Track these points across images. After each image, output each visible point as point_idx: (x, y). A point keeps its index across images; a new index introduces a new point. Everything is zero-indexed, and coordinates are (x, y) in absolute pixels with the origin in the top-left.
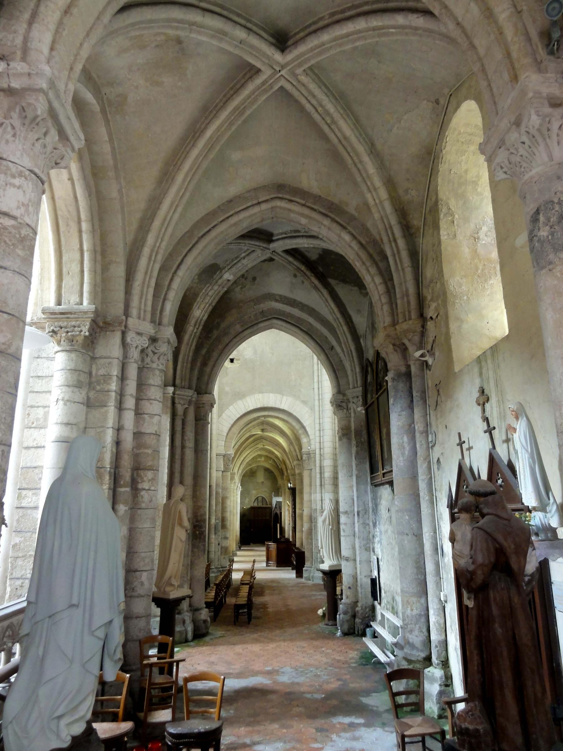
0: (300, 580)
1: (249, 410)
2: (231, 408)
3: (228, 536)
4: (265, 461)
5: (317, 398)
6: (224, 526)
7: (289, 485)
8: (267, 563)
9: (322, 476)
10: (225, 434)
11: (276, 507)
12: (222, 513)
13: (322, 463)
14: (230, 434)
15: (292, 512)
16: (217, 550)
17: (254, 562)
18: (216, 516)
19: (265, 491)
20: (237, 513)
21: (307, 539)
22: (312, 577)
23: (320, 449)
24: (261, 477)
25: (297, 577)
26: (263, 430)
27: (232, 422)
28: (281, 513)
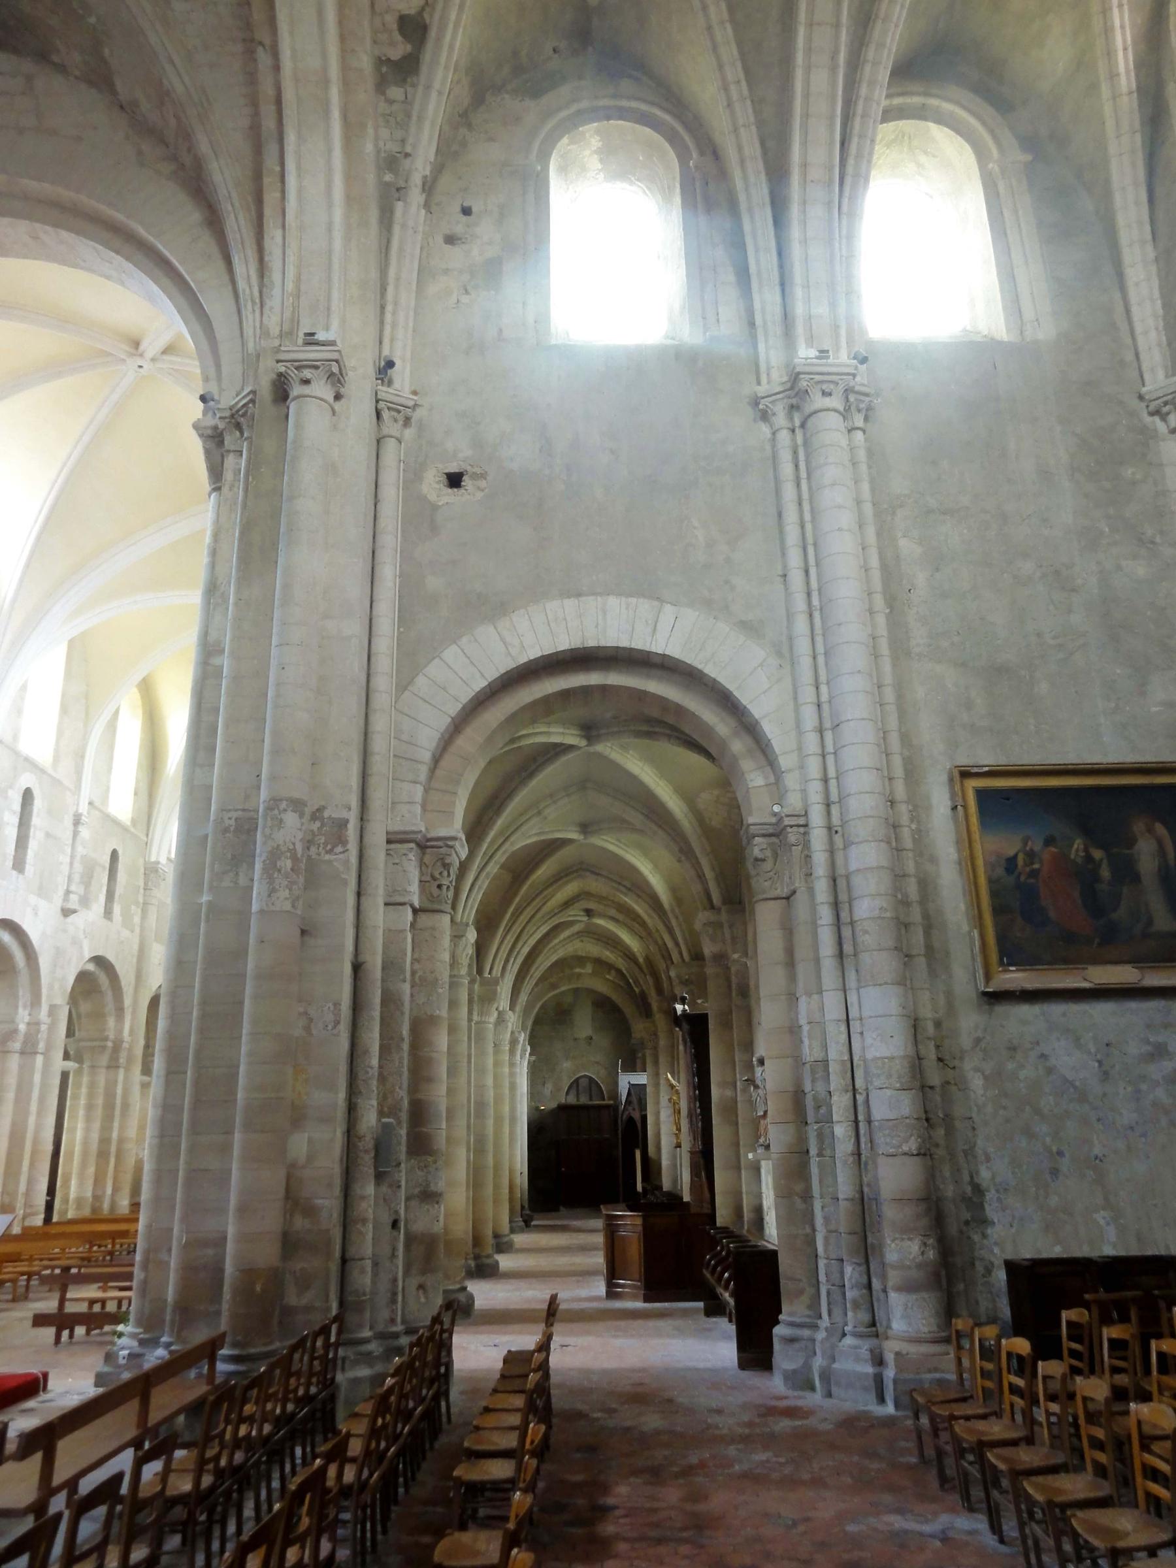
0: (754, 1379)
1: (523, 659)
2: (451, 653)
3: (440, 1185)
4: (594, 973)
7: (679, 1008)
8: (610, 1285)
9: (844, 915)
10: (427, 756)
11: (628, 1102)
13: (840, 861)
14: (446, 762)
15: (692, 1099)
17: (552, 1313)
18: (383, 1098)
20: (513, 1119)
22: (826, 1376)
23: (828, 805)
24: (584, 1024)
25: (743, 1365)
26: (585, 828)
27: (454, 709)
28: (644, 1118)
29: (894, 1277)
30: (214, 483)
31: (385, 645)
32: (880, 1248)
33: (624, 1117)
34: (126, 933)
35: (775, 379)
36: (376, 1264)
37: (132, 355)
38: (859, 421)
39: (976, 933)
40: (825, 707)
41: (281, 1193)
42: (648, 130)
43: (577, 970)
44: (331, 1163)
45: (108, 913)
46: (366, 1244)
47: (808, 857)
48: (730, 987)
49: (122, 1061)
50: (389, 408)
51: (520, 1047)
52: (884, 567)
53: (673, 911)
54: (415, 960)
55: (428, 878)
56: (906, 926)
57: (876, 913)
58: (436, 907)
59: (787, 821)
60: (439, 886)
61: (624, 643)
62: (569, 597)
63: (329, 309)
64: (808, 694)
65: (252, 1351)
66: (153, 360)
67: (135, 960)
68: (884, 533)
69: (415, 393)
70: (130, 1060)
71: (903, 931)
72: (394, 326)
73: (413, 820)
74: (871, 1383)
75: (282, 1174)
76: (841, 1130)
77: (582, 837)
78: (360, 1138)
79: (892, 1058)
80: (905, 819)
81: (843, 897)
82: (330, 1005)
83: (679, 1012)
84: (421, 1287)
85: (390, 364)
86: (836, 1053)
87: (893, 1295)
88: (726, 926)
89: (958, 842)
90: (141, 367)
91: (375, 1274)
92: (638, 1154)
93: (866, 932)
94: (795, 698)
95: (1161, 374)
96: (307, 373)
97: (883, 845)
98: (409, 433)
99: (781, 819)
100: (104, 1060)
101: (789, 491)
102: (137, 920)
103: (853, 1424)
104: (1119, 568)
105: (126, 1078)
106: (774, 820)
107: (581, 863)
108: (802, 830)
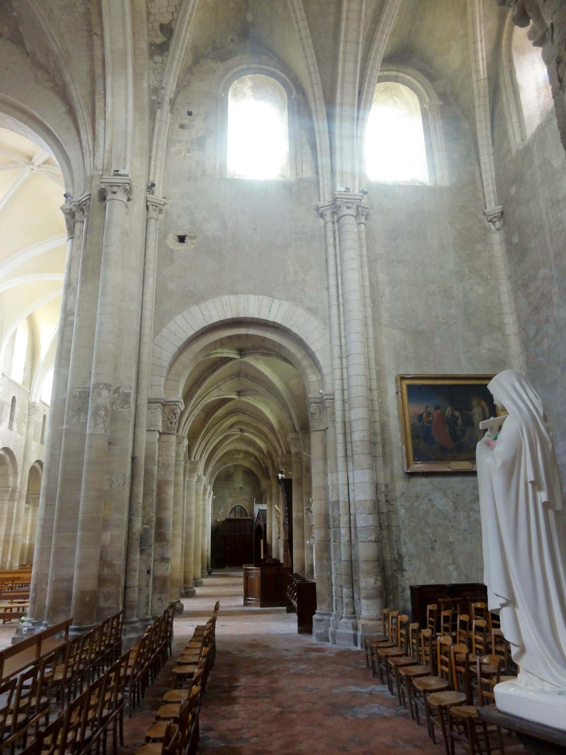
1: (211, 322)
2: (178, 318)
3: (169, 555)
4: (244, 458)
5: (334, 301)
6: (161, 537)
7: (280, 476)
8: (245, 600)
10: (166, 365)
11: (258, 517)
12: (158, 512)
14: (176, 366)
15: (285, 517)
16: (144, 583)
18: (144, 517)
19: (245, 500)
20: (204, 525)
21: (319, 559)
22: (334, 635)
23: (343, 390)
24: (239, 481)
25: (300, 632)
26: (239, 393)
27: (179, 343)
28: (265, 525)
29: (363, 593)
30: (70, 235)
31: (148, 313)
32: (358, 581)
33: (256, 524)
34: (19, 436)
35: (326, 199)
36: (140, 589)
37: (28, 164)
38: (363, 220)
39: (404, 447)
40: (343, 347)
41: (99, 558)
42: (274, 80)
43: (236, 456)
44: (121, 545)
45: (10, 427)
46: (135, 581)
47: (334, 413)
48: (302, 467)
49: (16, 497)
50: (152, 205)
51: (208, 492)
52: (371, 286)
53: (279, 431)
54: (159, 456)
55: (166, 419)
56: (374, 444)
57: (362, 438)
58: (168, 432)
59: (325, 397)
60: (171, 423)
61: (256, 316)
62: (232, 294)
63: (125, 159)
64: (336, 342)
65: (85, 626)
66: (39, 166)
67: (23, 449)
68: (371, 270)
69: (164, 198)
70: (20, 497)
71: (373, 446)
72: (155, 166)
73: (160, 393)
74: (352, 638)
75: (99, 551)
76: (344, 531)
77: (238, 397)
78: (134, 534)
79: (365, 501)
80: (376, 397)
81: (348, 431)
82: (121, 475)
83: (280, 478)
84: (159, 599)
85: (153, 185)
86: (343, 498)
87: (363, 601)
88: (301, 440)
89: (398, 408)
90: (32, 169)
91: (139, 594)
92: (262, 541)
93: (357, 446)
94: (331, 343)
95: (493, 204)
96: (115, 189)
97: (366, 409)
98: (161, 216)
99: (323, 396)
100: (7, 497)
101: (331, 250)
102: (24, 430)
103: (343, 655)
104: (472, 289)
105: (18, 505)
106: (320, 396)
107: (238, 409)
108: (332, 401)
